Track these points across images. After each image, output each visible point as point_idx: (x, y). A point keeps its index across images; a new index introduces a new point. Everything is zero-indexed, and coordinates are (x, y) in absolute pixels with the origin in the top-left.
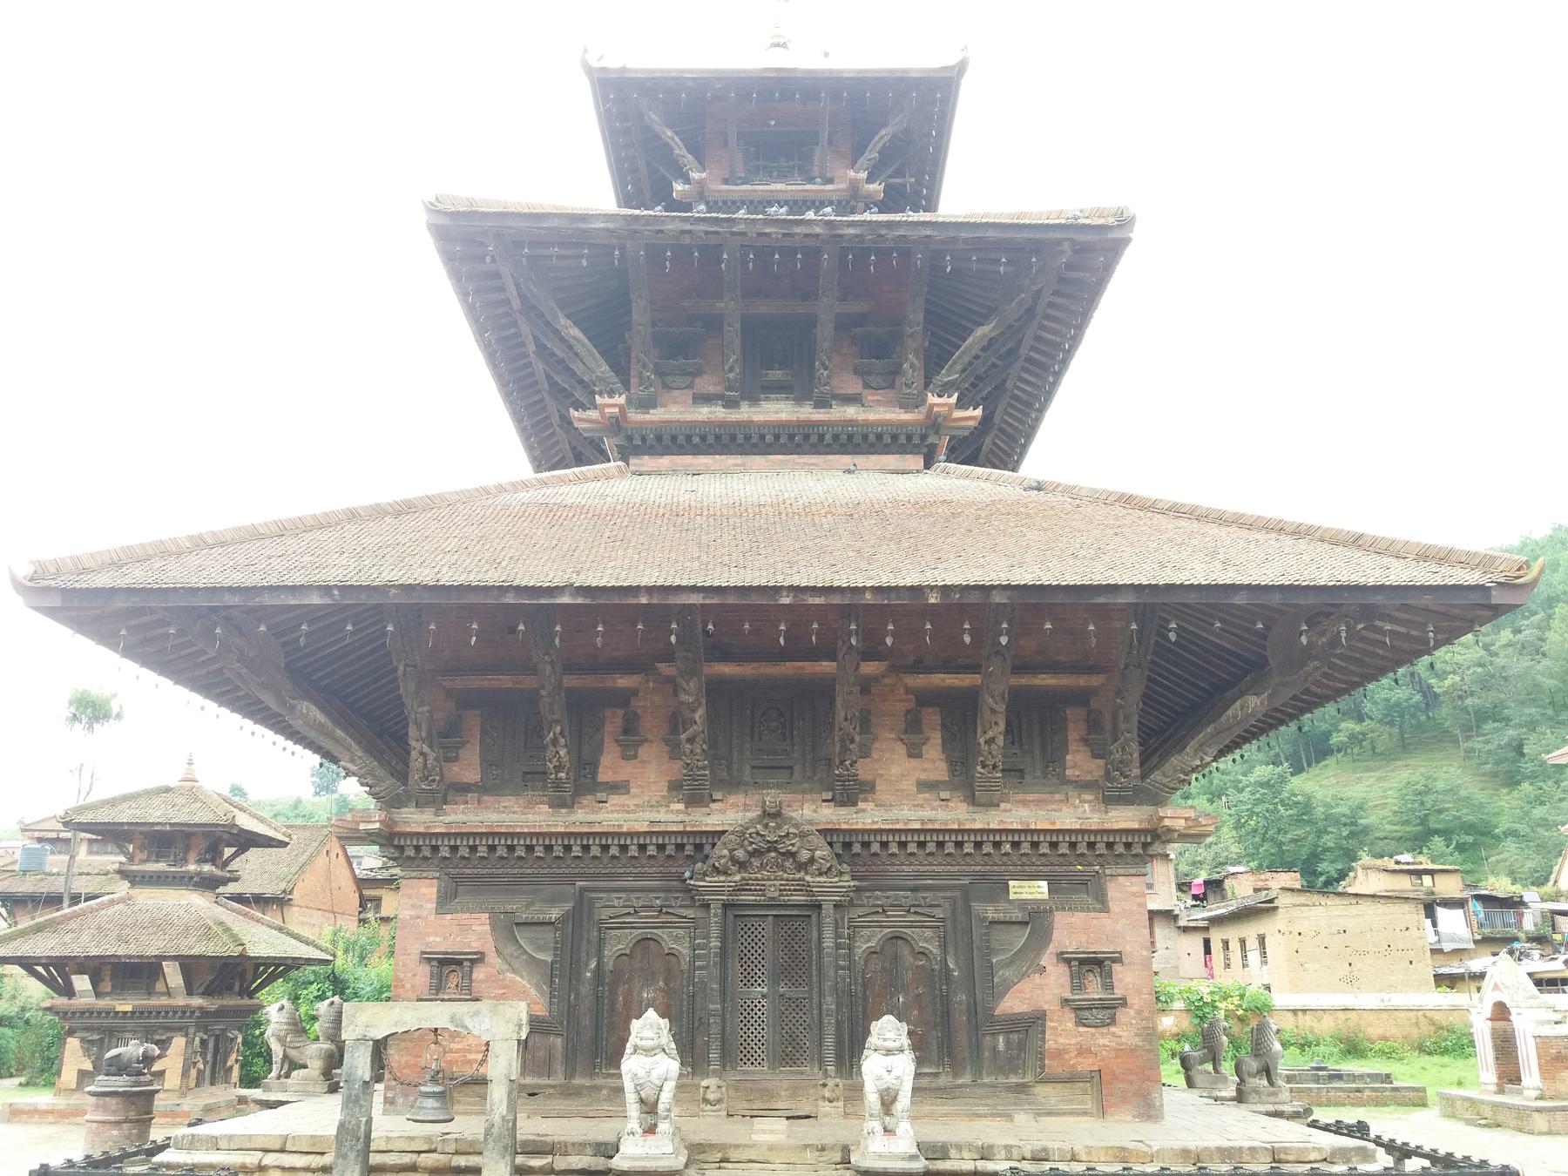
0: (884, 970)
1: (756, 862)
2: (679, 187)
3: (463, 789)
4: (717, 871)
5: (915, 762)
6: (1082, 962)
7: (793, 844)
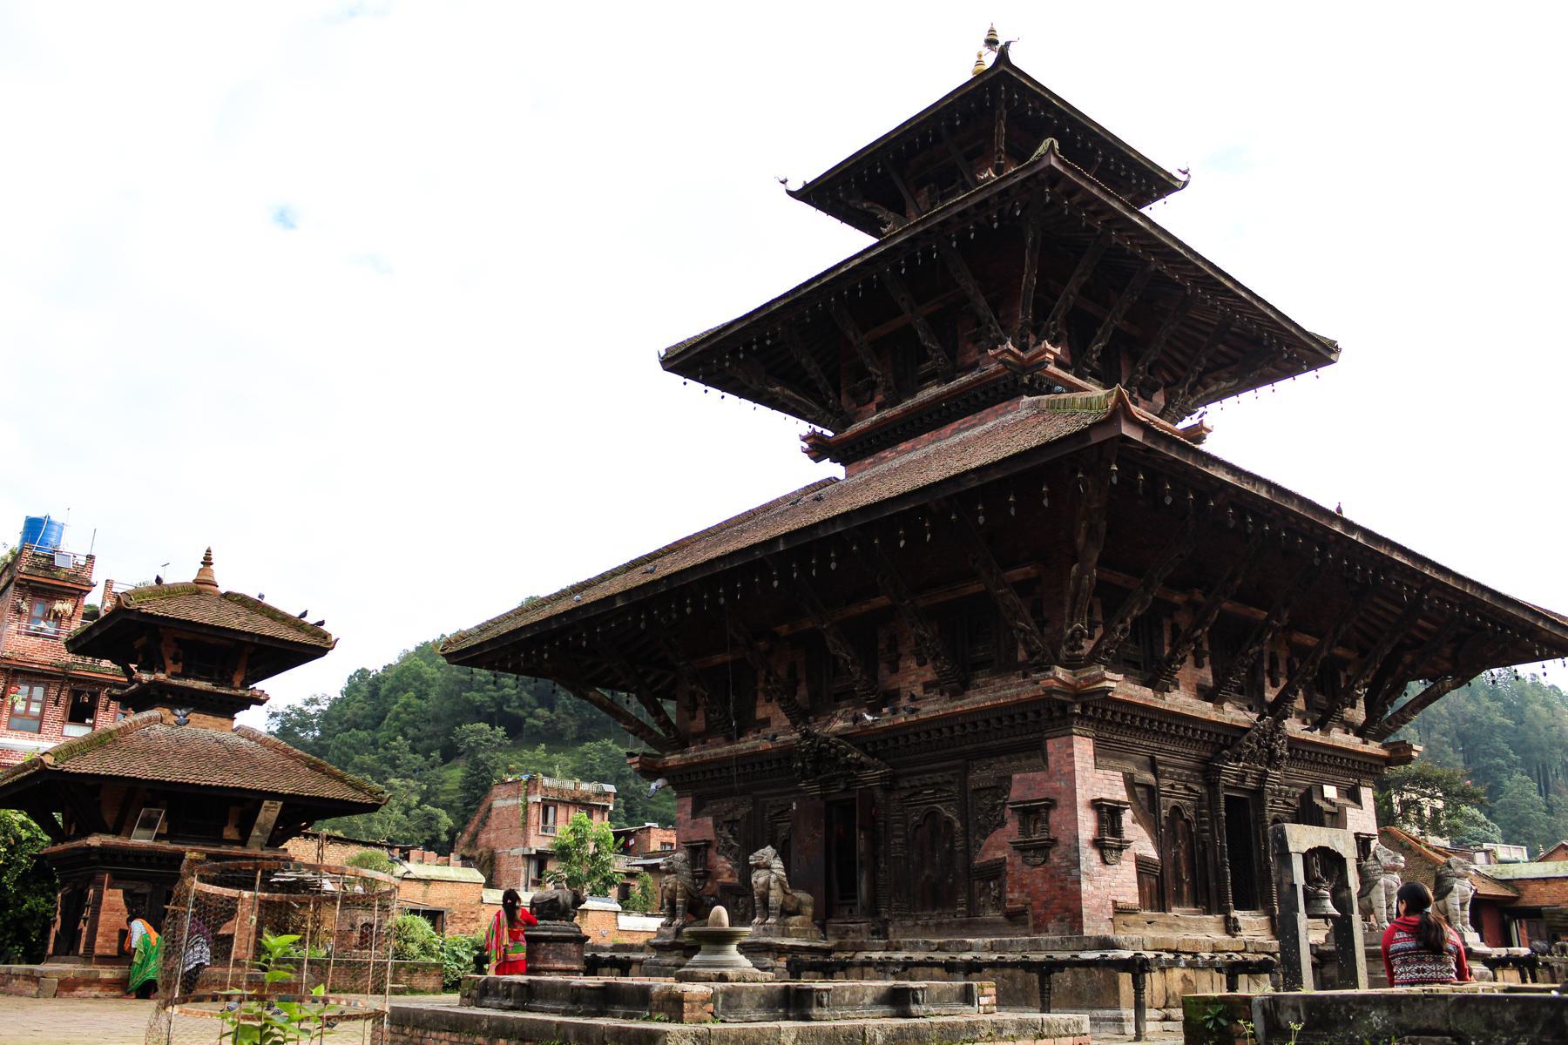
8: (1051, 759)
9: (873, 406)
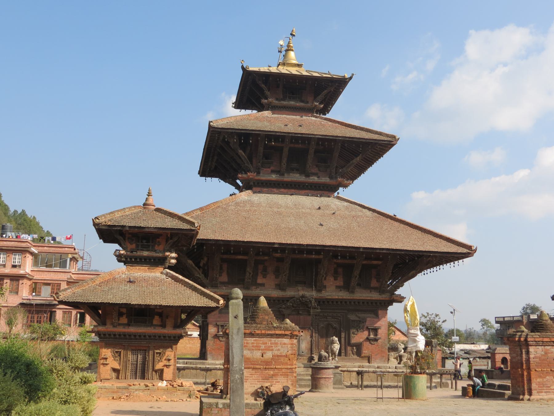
2: (264, 101)
3: (223, 283)
6: (372, 329)
8: (380, 316)
9: (269, 170)
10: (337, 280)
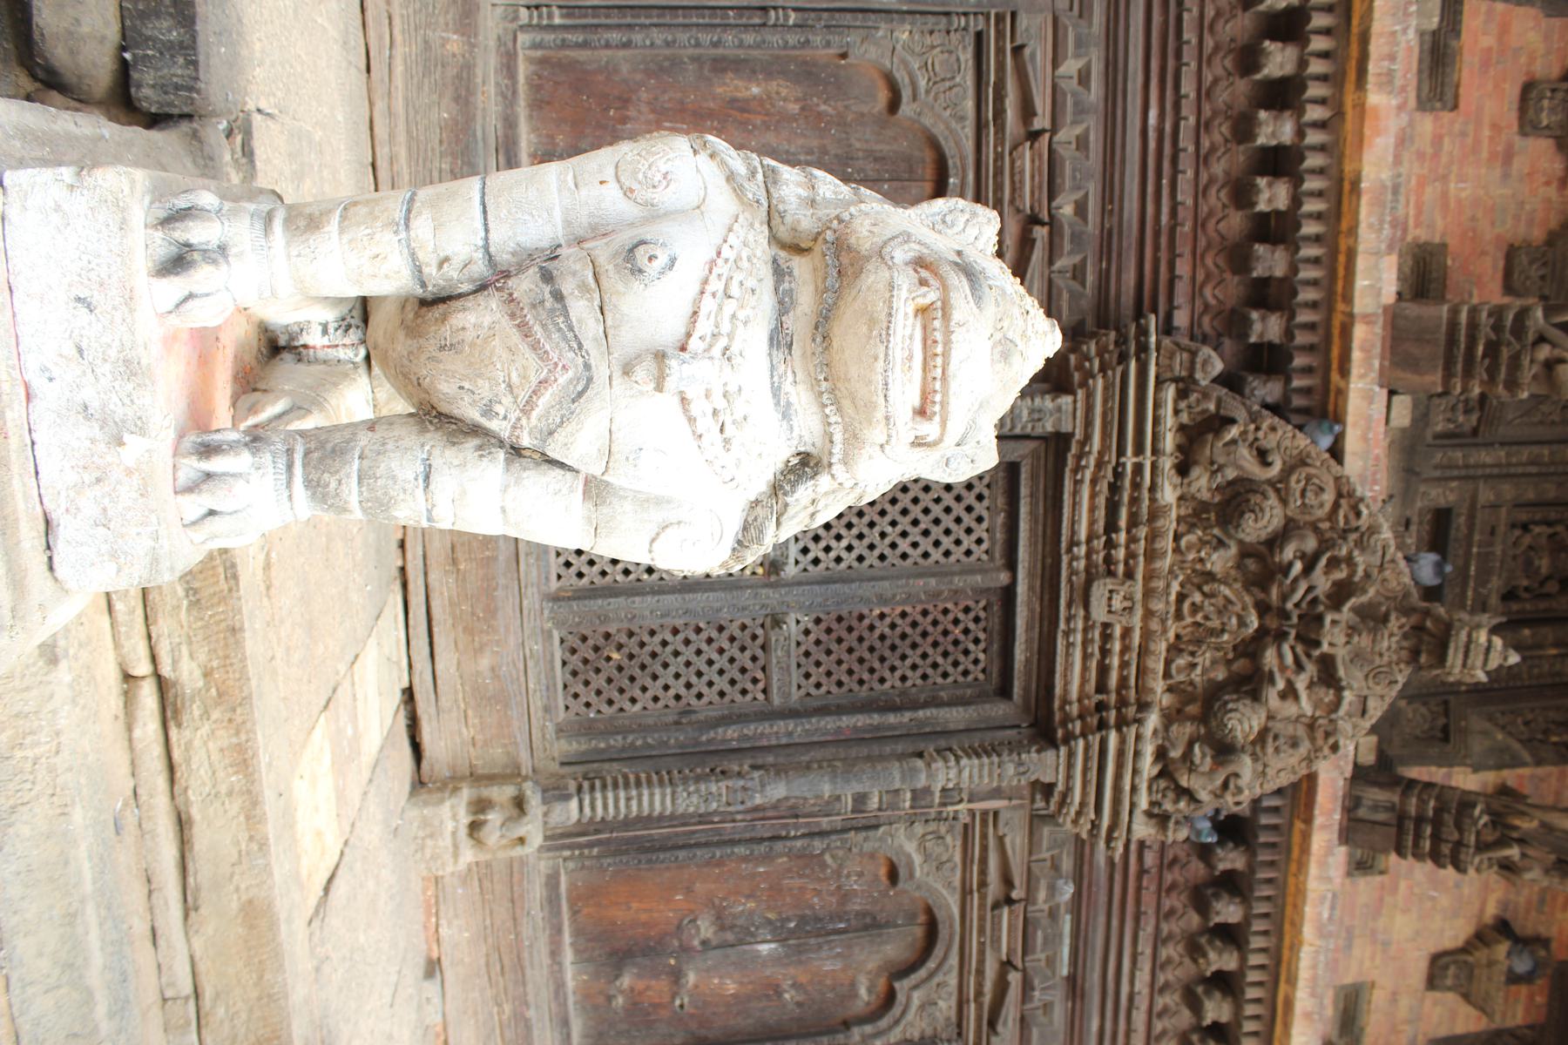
0: (845, 897)
1: (1220, 561)
4: (1199, 434)
5: (1418, 969)
7: (1291, 701)
10: (1432, 982)
